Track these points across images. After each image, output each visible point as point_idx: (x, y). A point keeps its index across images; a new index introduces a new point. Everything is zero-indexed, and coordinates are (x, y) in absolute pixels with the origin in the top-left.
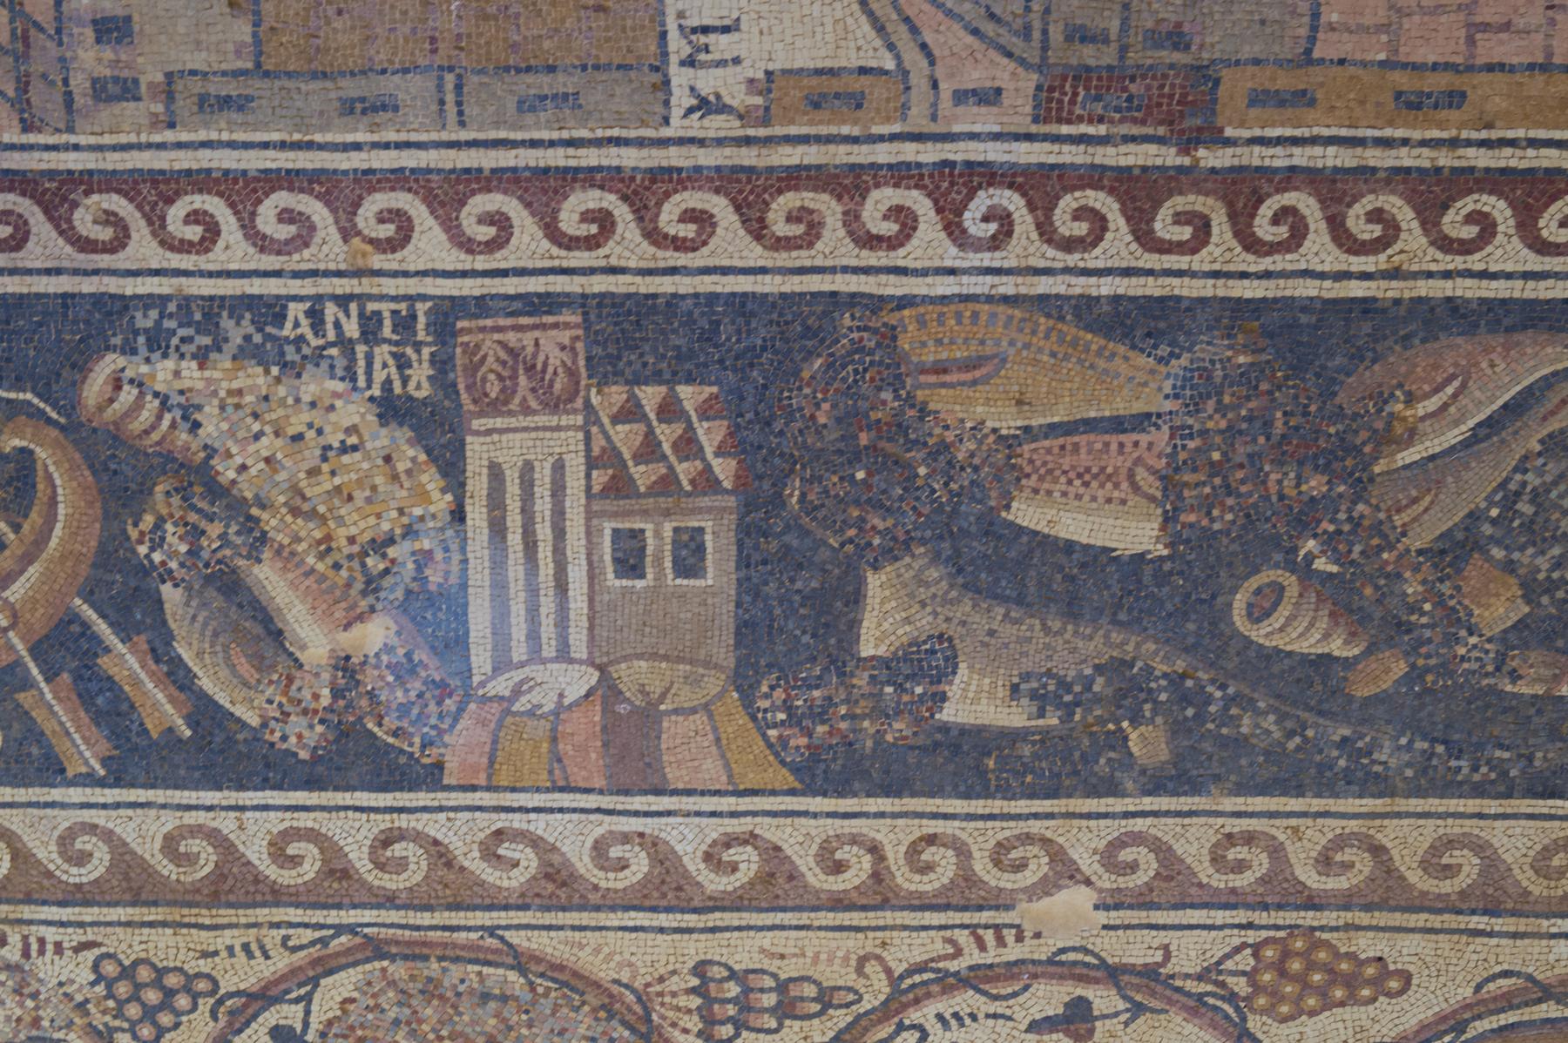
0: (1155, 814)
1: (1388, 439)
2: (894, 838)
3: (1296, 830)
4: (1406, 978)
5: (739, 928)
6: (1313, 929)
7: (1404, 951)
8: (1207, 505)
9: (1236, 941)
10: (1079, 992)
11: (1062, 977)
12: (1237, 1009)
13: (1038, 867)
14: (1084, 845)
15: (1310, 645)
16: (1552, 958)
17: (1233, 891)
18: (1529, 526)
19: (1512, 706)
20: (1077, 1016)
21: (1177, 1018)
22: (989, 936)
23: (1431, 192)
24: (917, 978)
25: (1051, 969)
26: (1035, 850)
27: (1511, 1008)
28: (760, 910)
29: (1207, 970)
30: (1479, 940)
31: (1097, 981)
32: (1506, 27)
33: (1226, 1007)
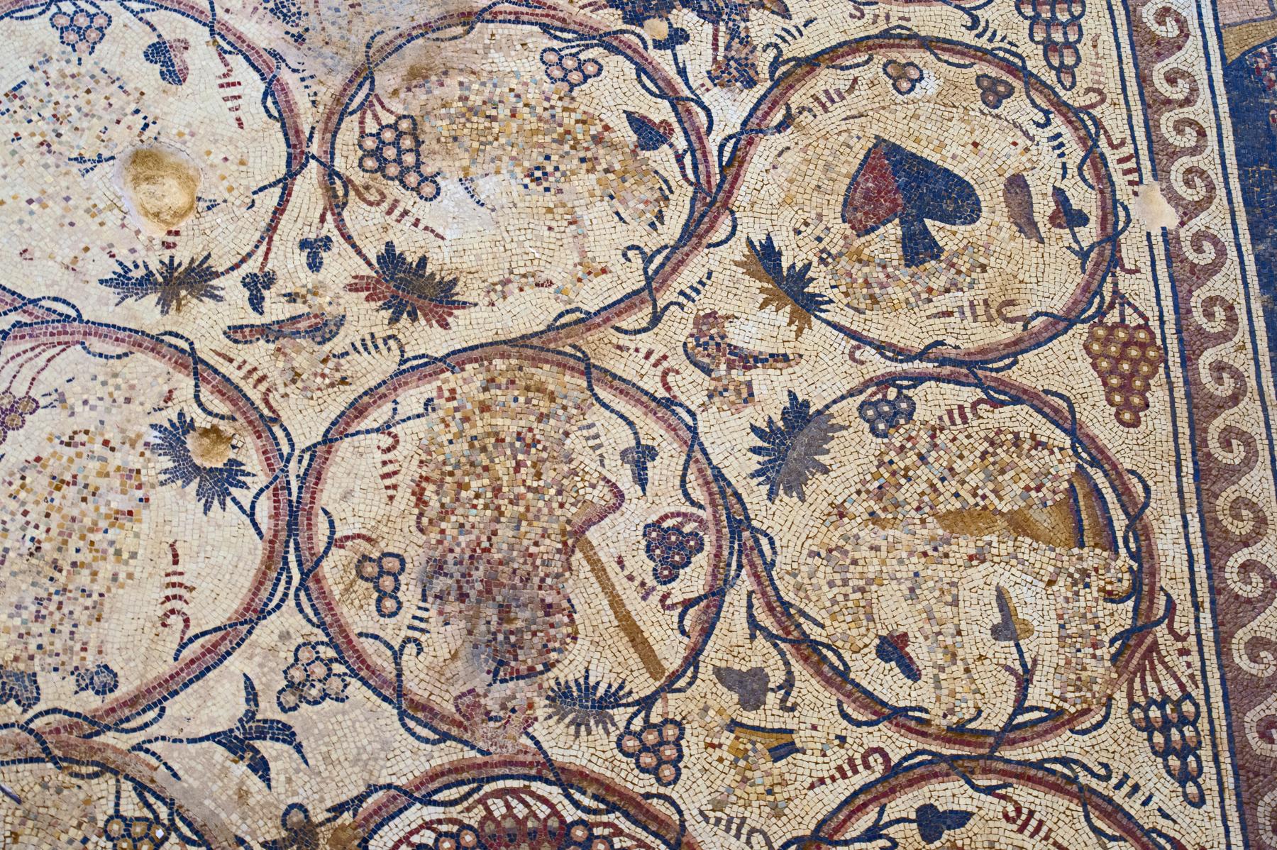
0: (1242, 263)
2: (1201, 111)
3: (1243, 347)
4: (1136, 423)
5: (1114, 23)
6: (1166, 362)
7: (1157, 420)
9: (1149, 314)
11: (1103, 208)
12: (1092, 317)
13: (1189, 195)
14: (1214, 219)
16: (1166, 518)
17: (1189, 311)
20: (1068, 216)
21: (1080, 279)
22: (1132, 164)
24: (1089, 123)
25: (1109, 202)
26: (1203, 192)
27: (1118, 496)
28: (1130, 36)
29: (1123, 297)
30: (1173, 469)
31: (1103, 228)
33: (1093, 310)
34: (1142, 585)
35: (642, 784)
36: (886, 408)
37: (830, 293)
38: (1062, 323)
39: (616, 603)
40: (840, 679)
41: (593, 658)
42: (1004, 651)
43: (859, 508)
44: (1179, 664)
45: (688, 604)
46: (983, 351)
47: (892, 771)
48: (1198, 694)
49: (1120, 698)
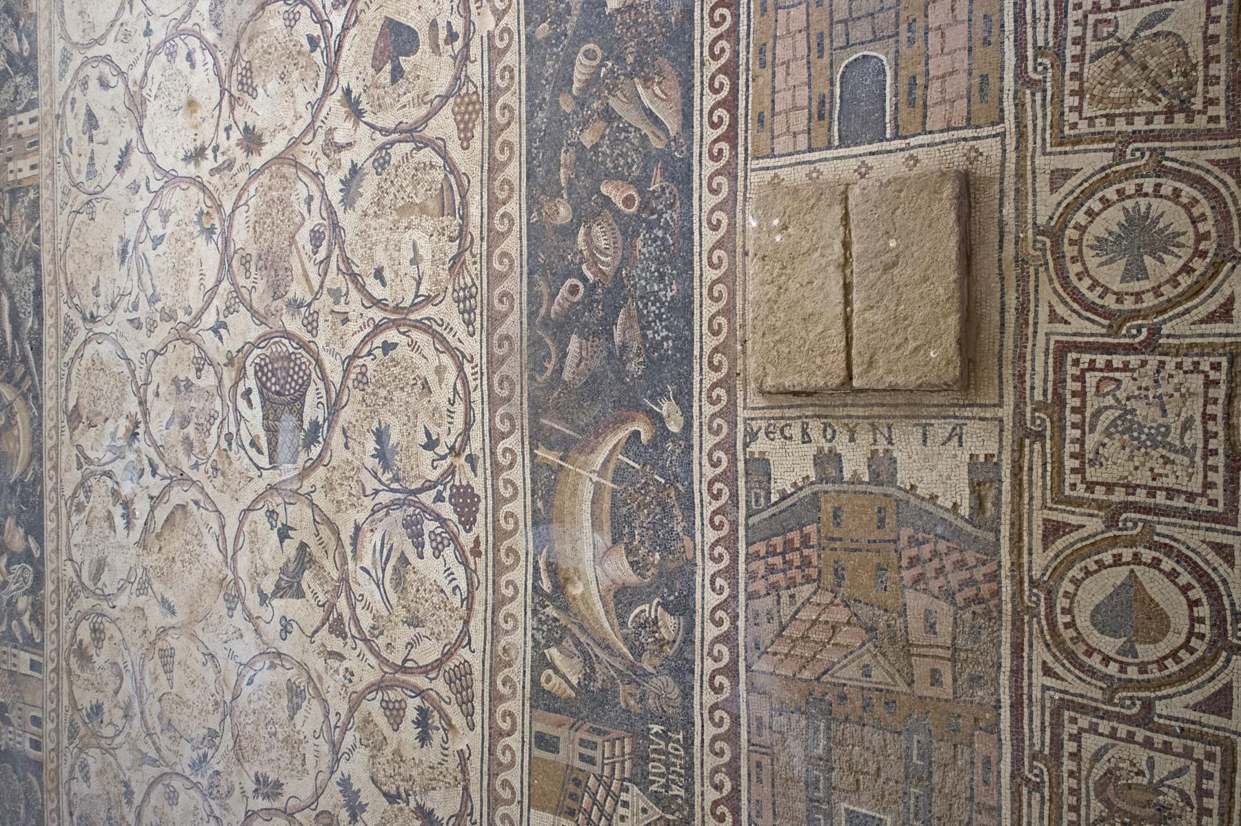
1: (647, 81)
7: (476, 144)
8: (623, 23)
10: (461, 35)
14: (509, 20)
15: (577, 76)
18: (617, 139)
19: (557, 154)
23: (730, 70)
32: (788, 74)
34: (462, 233)
35: (307, 337)
36: (381, 160)
37: (367, 107)
38: (445, 98)
39: (303, 265)
40: (362, 289)
41: (297, 290)
42: (412, 270)
43: (371, 212)
44: (471, 268)
45: (321, 262)
46: (416, 122)
47: (376, 327)
48: (478, 283)
49: (450, 287)
